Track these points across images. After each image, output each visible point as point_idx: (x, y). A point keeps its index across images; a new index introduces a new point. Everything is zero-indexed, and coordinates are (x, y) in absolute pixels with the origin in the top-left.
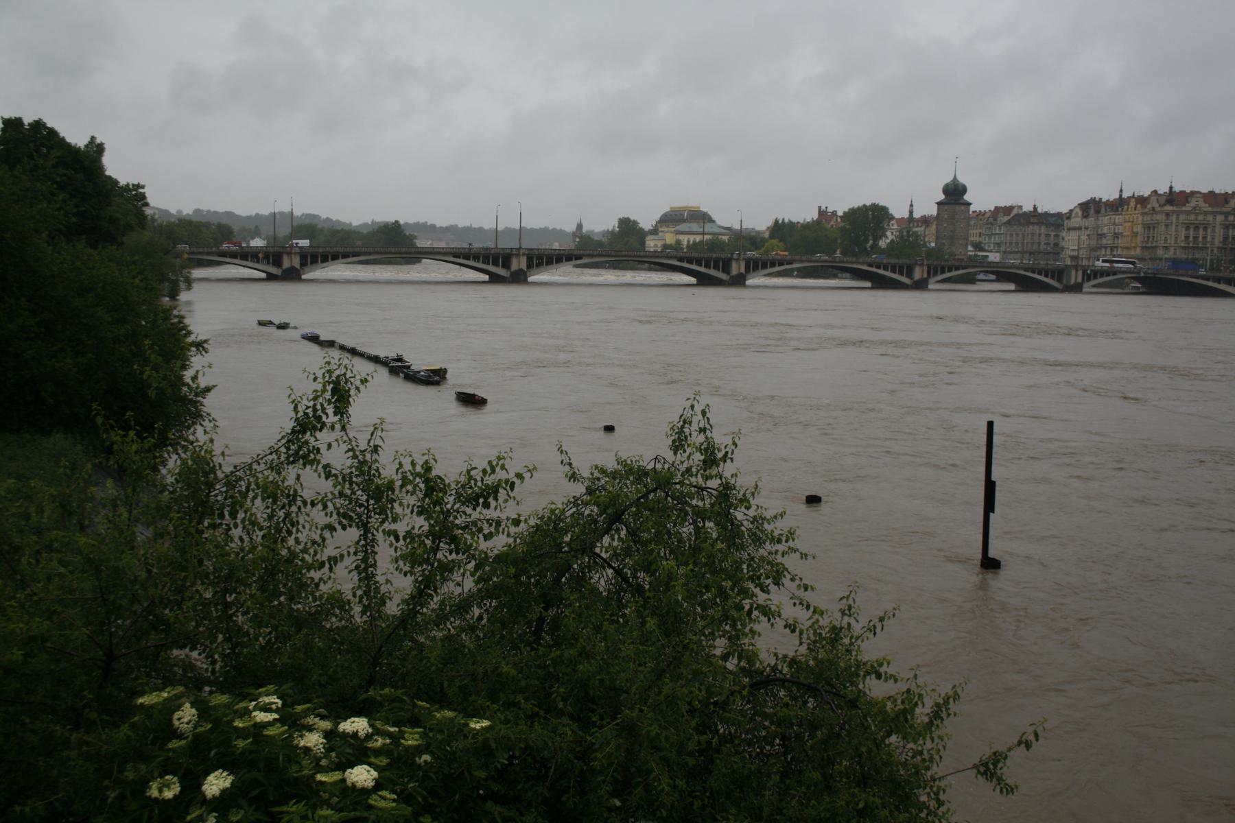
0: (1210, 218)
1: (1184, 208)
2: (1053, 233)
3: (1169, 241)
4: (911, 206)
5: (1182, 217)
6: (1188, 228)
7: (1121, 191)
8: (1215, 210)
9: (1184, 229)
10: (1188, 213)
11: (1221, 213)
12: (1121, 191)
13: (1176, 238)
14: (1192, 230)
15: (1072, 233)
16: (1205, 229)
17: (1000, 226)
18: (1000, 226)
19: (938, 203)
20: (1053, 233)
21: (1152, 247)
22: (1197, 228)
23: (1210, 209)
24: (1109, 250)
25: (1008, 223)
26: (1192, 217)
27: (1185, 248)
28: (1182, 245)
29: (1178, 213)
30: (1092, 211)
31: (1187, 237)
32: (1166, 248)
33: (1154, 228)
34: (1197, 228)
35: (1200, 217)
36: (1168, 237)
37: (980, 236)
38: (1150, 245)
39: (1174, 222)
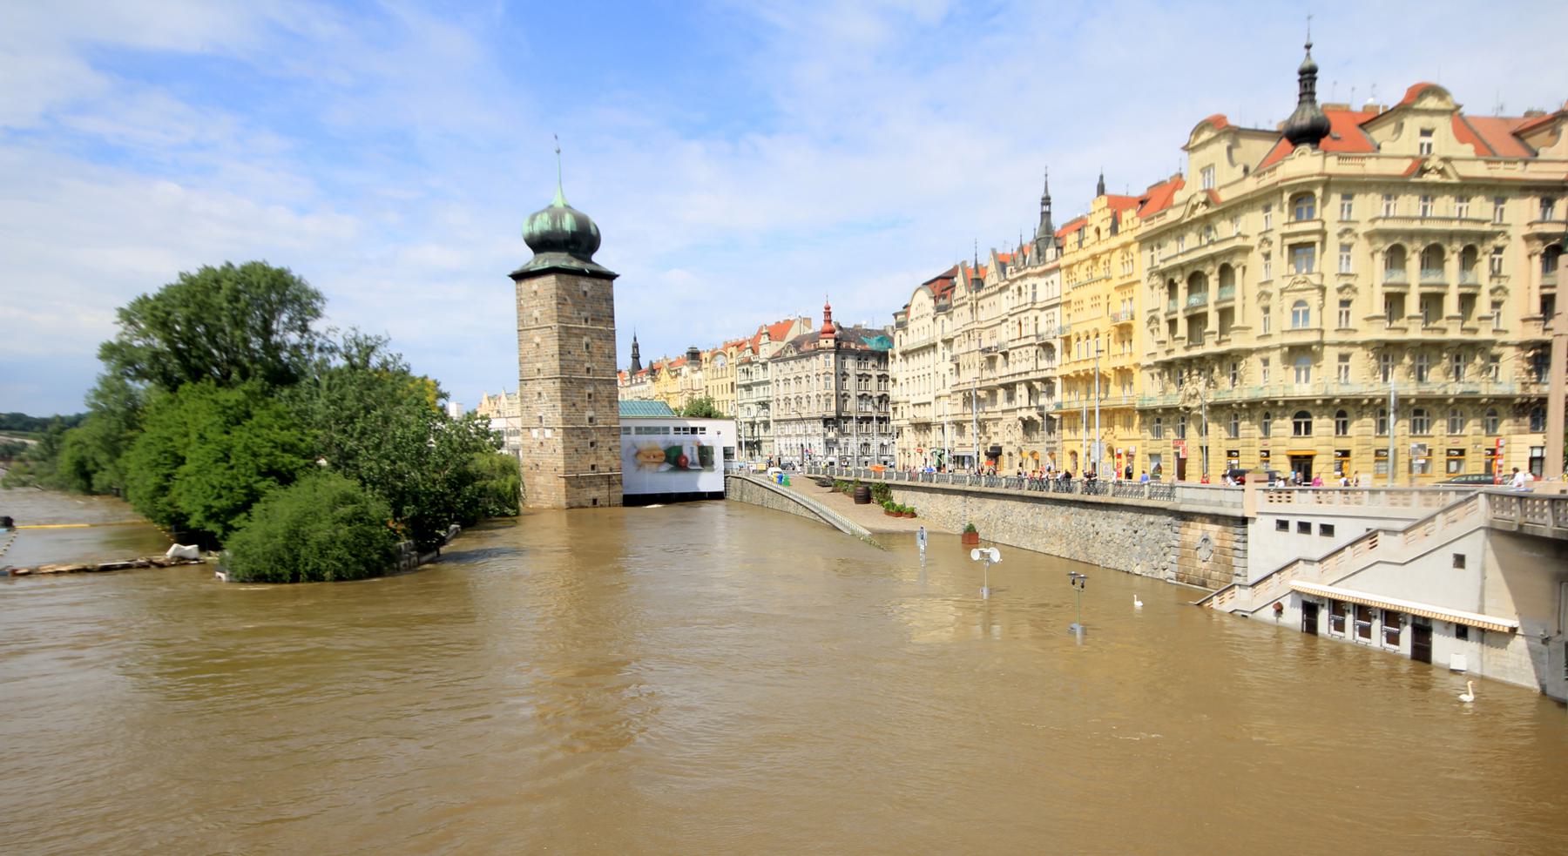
0: (1480, 207)
1: (1372, 167)
2: (875, 373)
3: (1314, 322)
4: (636, 347)
5: (1367, 207)
6: (1396, 256)
7: (1046, 201)
8: (1502, 171)
9: (1380, 260)
10: (1390, 187)
11: (1526, 188)
12: (1046, 201)
13: (1345, 303)
14: (1414, 262)
15: (916, 362)
16: (1469, 257)
17: (764, 365)
18: (764, 365)
19: (519, 277)
20: (875, 373)
21: (1221, 358)
22: (1433, 257)
23: (1480, 170)
24: (1022, 391)
25: (776, 359)
26: (1408, 204)
27: (1386, 352)
28: (1381, 333)
29: (1349, 187)
30: (961, 290)
31: (1394, 301)
32: (1300, 354)
33: (1226, 273)
34: (1433, 257)
35: (1444, 206)
36: (1313, 298)
37: (732, 390)
38: (1210, 347)
39: (1333, 229)
